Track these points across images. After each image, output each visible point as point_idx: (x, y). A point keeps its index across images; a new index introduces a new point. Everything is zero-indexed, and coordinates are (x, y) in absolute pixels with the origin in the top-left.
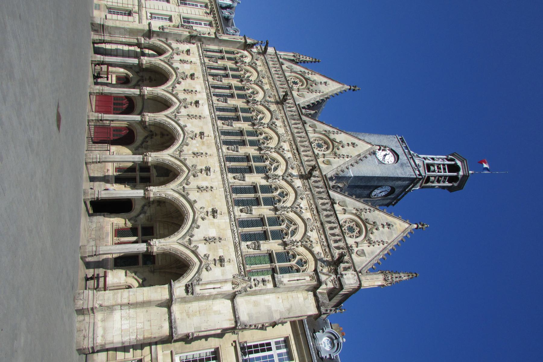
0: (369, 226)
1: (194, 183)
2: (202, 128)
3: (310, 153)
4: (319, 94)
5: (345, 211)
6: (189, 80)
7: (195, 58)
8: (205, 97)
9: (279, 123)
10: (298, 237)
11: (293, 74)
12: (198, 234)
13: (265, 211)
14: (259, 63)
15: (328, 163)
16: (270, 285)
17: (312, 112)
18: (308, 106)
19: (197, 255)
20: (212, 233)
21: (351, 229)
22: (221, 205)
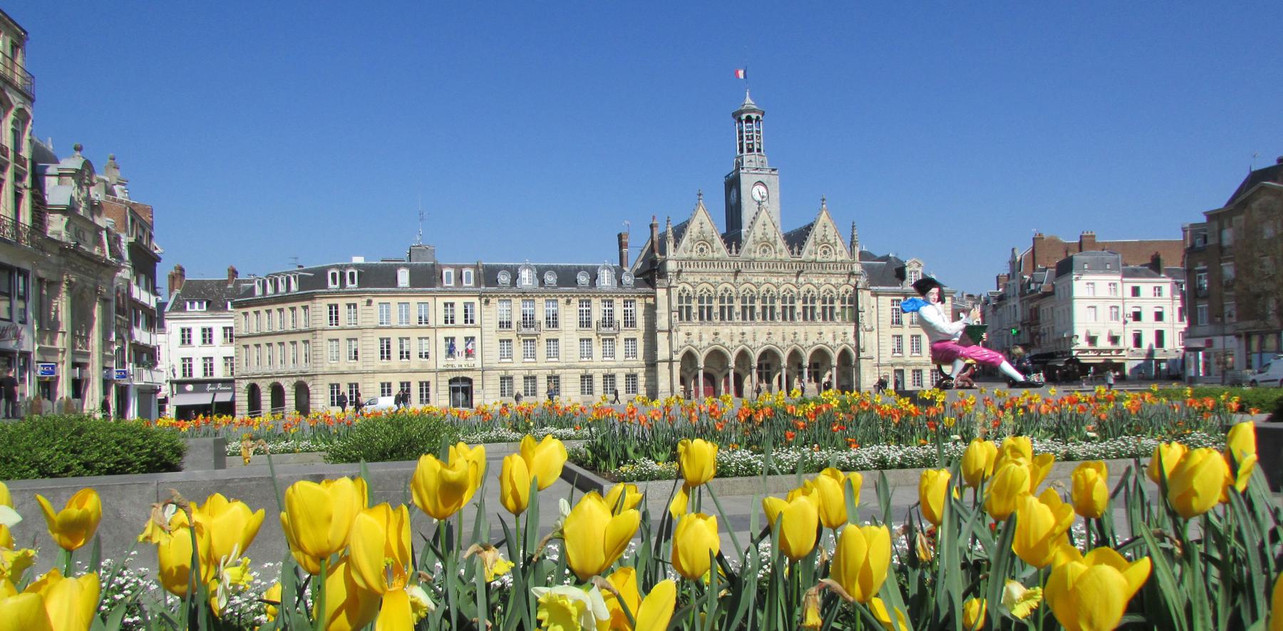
0: (826, 241)
1: (802, 342)
2: (763, 333)
3: (779, 265)
4: (715, 234)
5: (816, 253)
6: (719, 336)
7: (695, 330)
8: (735, 327)
9: (755, 280)
10: (834, 290)
11: (694, 249)
12: (831, 343)
13: (818, 305)
14: (691, 279)
15: (781, 251)
16: (864, 314)
17: (734, 246)
18: (727, 247)
19: (841, 345)
20: (831, 335)
21: (825, 252)
22: (815, 329)
